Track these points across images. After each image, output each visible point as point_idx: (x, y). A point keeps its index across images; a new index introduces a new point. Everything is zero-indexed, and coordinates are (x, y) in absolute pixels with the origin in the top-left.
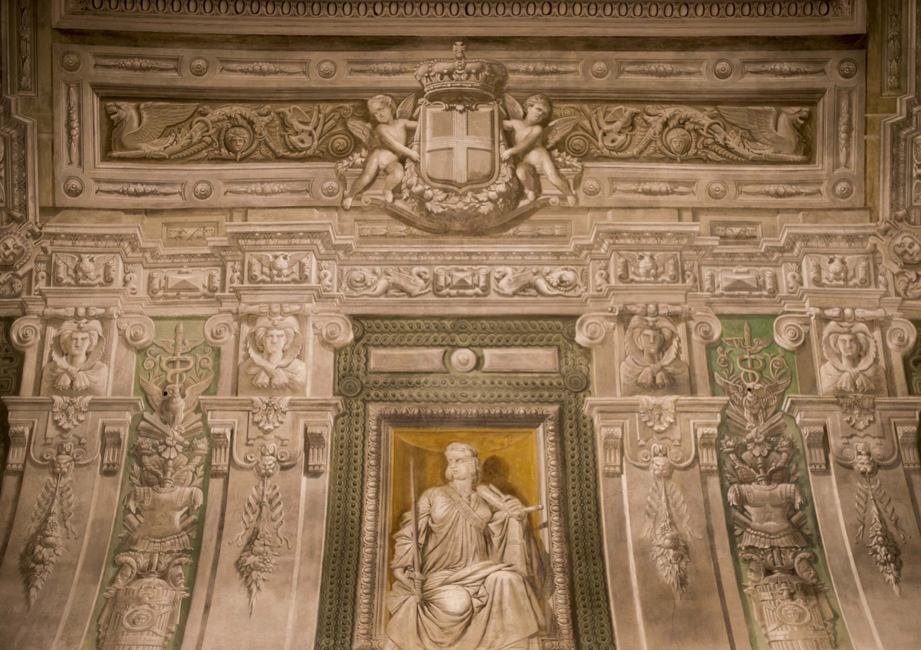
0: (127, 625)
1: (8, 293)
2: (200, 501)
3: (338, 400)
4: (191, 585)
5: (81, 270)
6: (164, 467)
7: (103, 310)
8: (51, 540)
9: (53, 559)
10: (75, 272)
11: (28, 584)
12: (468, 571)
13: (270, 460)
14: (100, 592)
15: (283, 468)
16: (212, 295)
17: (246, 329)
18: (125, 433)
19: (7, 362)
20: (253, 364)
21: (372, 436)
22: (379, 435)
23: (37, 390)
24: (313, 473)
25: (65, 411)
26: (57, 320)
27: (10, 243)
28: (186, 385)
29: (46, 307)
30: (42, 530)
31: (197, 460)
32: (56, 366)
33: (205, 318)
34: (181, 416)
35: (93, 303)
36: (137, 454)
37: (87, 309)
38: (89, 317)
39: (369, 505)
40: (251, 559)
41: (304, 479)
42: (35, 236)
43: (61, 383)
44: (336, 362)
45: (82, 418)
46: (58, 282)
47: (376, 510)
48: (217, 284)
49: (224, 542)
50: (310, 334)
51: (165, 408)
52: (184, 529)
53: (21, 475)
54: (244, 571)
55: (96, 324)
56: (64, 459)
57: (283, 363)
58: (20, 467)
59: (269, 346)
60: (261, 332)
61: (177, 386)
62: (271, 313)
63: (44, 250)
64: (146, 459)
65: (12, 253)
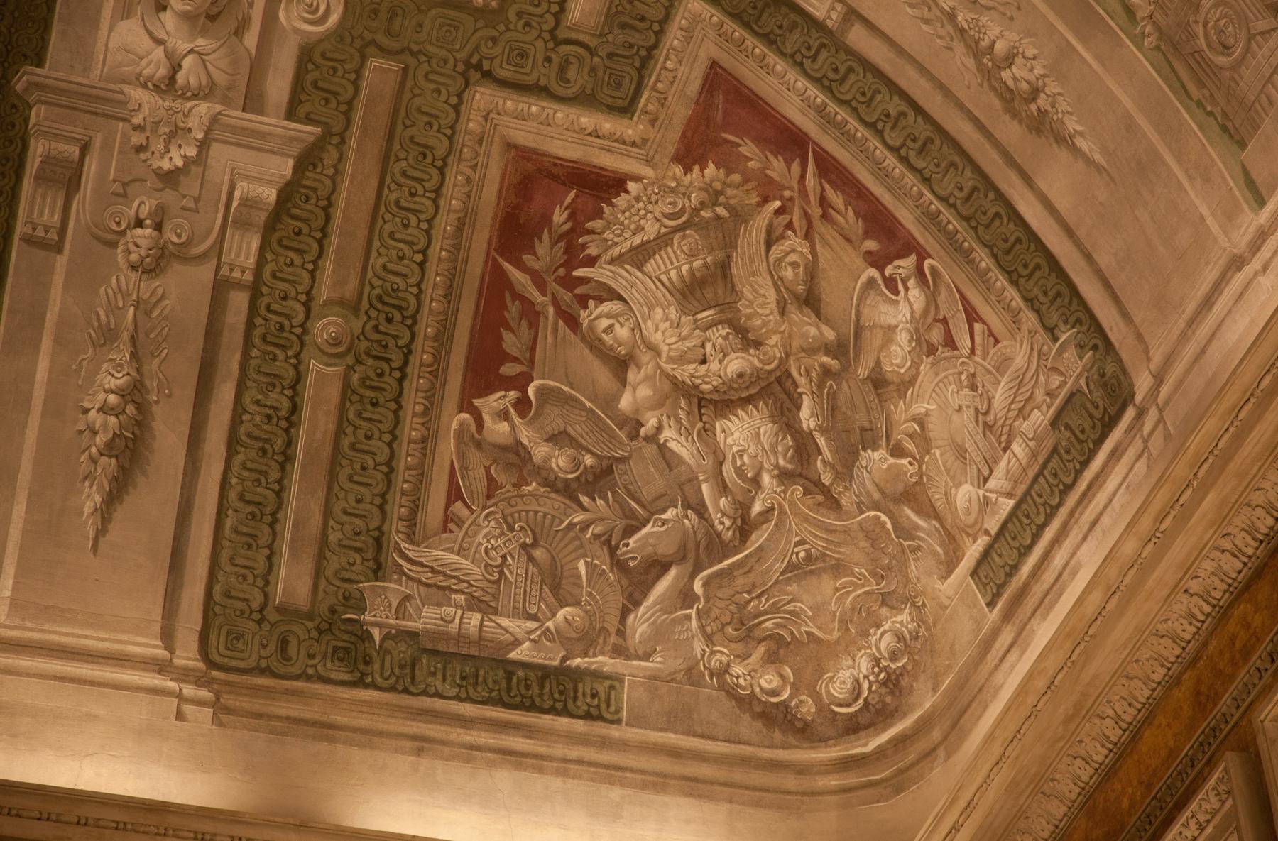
0: (1222, 60)
9: (1039, 71)
11: (1064, 140)
14: (1140, 48)
30: (977, 51)
53: (853, 15)
58: (839, 7)
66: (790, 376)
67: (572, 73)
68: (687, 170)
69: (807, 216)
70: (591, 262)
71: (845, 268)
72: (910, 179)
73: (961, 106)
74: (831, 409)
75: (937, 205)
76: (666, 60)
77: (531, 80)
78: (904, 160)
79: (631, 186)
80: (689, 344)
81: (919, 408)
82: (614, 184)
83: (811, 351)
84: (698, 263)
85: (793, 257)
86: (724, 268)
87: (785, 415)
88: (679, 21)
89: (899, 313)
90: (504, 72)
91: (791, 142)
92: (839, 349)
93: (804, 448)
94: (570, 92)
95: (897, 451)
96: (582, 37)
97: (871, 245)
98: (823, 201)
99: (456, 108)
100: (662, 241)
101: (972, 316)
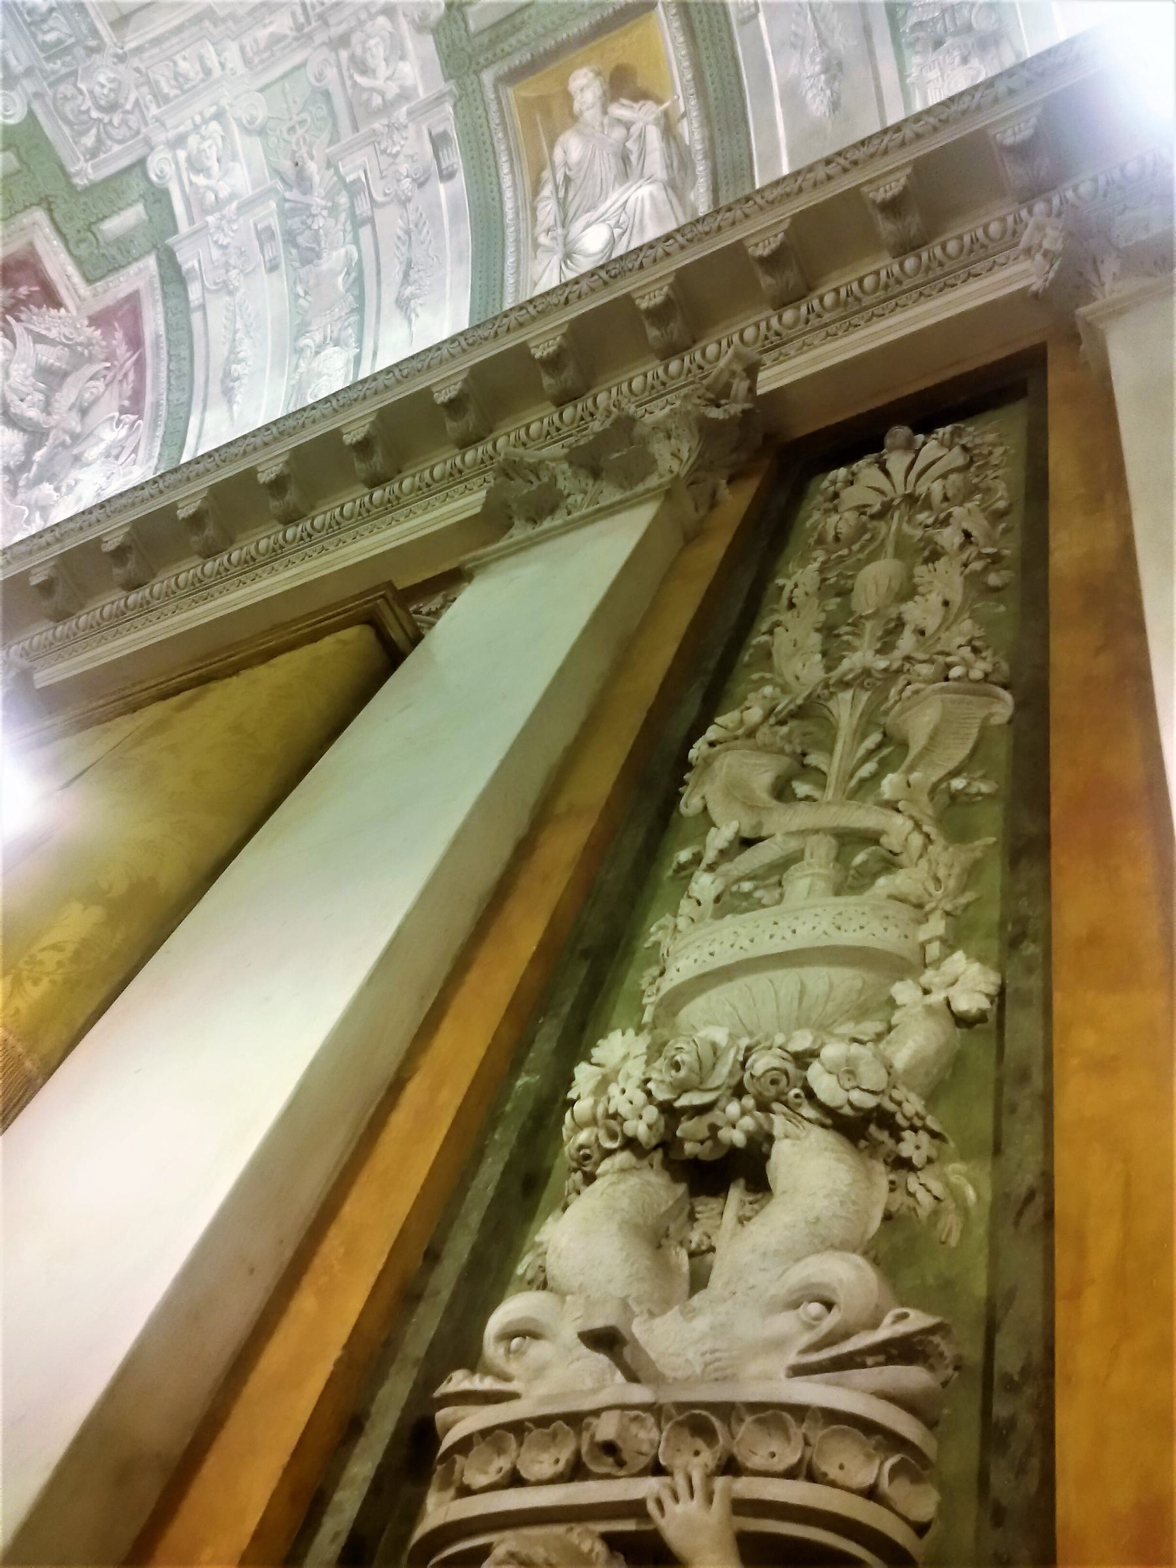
1: (128, 135)
2: (356, 256)
3: (451, 85)
4: (360, 341)
5: (181, 75)
6: (316, 239)
7: (215, 108)
8: (241, 355)
10: (176, 80)
11: (230, 403)
12: (609, 203)
13: (406, 183)
15: (421, 185)
16: (302, 36)
17: (344, 55)
18: (275, 223)
19: (158, 205)
20: (364, 89)
21: (493, 107)
22: (499, 102)
23: (191, 221)
24: (447, 176)
25: (219, 228)
26: (180, 141)
27: (102, 79)
28: (311, 146)
29: (167, 131)
30: (233, 351)
31: (343, 217)
32: (198, 187)
33: (303, 65)
34: (316, 179)
35: (204, 105)
36: (290, 238)
37: (201, 114)
38: (206, 122)
39: (507, 181)
40: (409, 290)
41: (442, 188)
42: (121, 59)
43: (208, 202)
44: (438, 44)
45: (235, 227)
46: (167, 99)
47: (514, 184)
48: (302, 19)
49: (384, 286)
50: (405, 27)
51: (301, 180)
52: (347, 291)
53: (203, 307)
54: (403, 305)
55: (214, 126)
56: (233, 273)
57: (389, 72)
59: (371, 63)
60: (358, 51)
61: (304, 151)
62: (361, 23)
63: (137, 70)
64: (300, 240)
65: (111, 90)
66: (48, 435)
67: (83, 246)
68: (89, 326)
69: (114, 377)
70: (18, 320)
71: (109, 406)
72: (164, 386)
73: (207, 368)
74: (50, 459)
75: (164, 402)
76: (122, 276)
77: (64, 230)
78: (169, 377)
79: (63, 310)
80: (24, 389)
81: (80, 477)
82: (57, 303)
83: (65, 431)
84: (58, 364)
85: (94, 390)
86: (66, 374)
87: (30, 449)
88: (140, 264)
89: (110, 435)
90: (58, 216)
91: (135, 342)
92: (76, 438)
93: (25, 466)
94: (75, 252)
95: (57, 489)
96: (99, 237)
97: (126, 403)
98: (126, 375)
99: (26, 207)
100: (52, 342)
101: (135, 450)
